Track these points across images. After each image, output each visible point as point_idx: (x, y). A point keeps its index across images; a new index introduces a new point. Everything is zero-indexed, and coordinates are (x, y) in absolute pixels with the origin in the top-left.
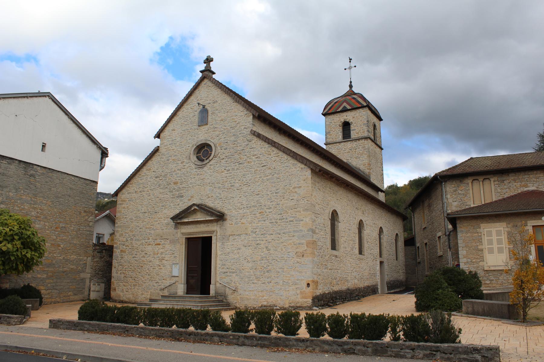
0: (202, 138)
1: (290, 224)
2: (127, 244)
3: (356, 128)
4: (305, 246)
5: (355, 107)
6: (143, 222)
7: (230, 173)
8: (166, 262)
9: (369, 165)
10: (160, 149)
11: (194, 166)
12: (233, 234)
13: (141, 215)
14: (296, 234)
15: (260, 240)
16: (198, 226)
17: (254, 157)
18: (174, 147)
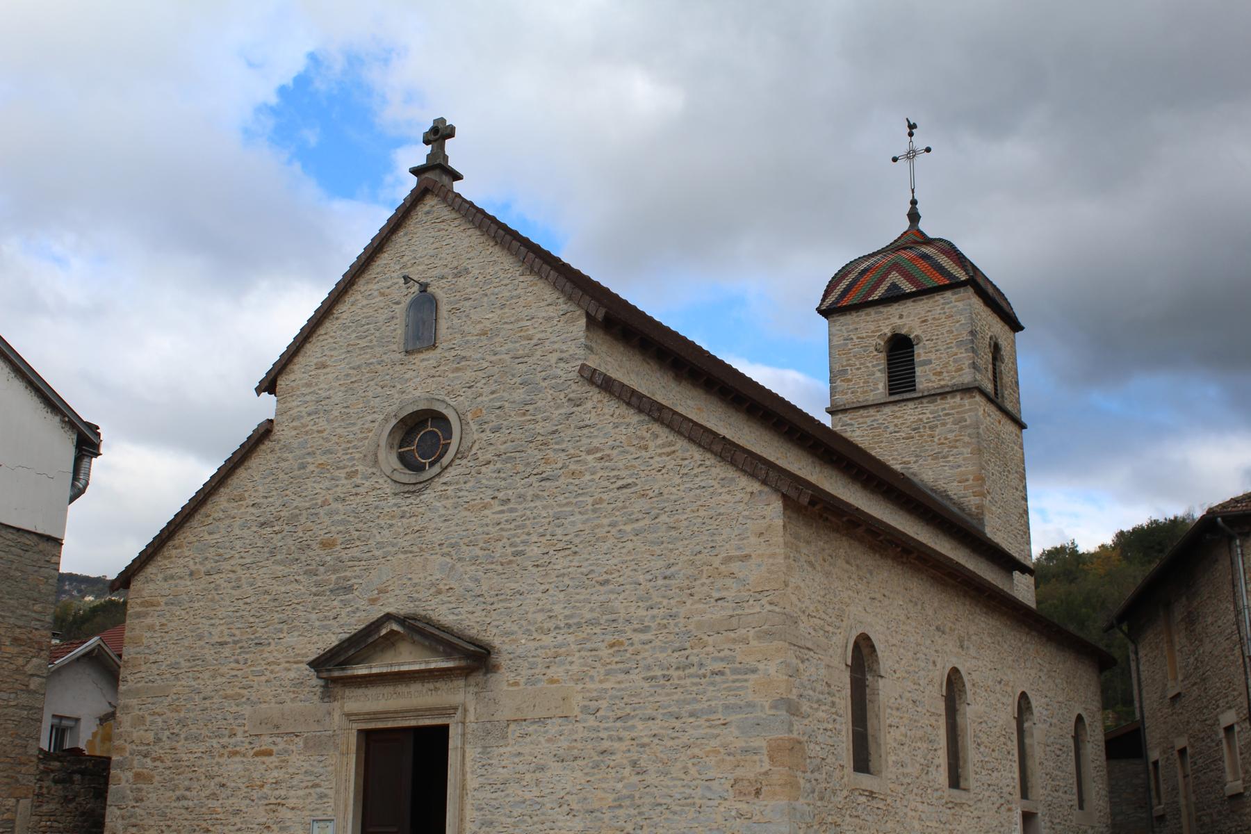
0: (417, 393)
1: (712, 684)
2: (157, 751)
4: (766, 759)
5: (930, 284)
6: (214, 677)
7: (512, 510)
8: (289, 814)
9: (980, 479)
10: (276, 428)
11: (388, 488)
12: (519, 716)
13: (209, 653)
14: (733, 718)
15: (610, 738)
16: (402, 689)
17: (590, 458)
18: (322, 424)
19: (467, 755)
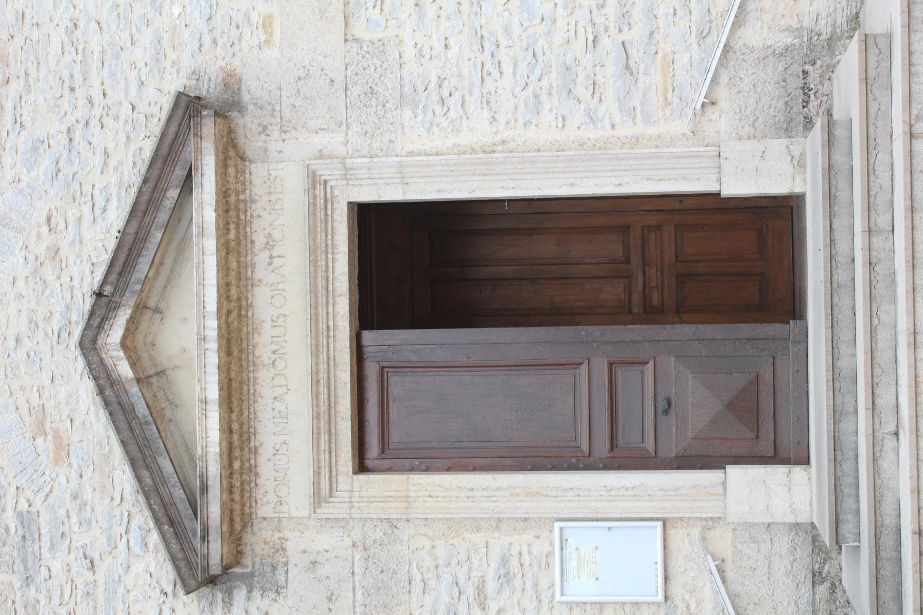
16: (264, 344)
19: (417, 147)
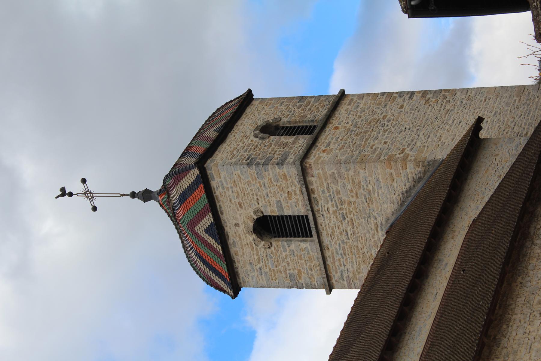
3: (273, 200)
5: (204, 201)
9: (391, 159)
